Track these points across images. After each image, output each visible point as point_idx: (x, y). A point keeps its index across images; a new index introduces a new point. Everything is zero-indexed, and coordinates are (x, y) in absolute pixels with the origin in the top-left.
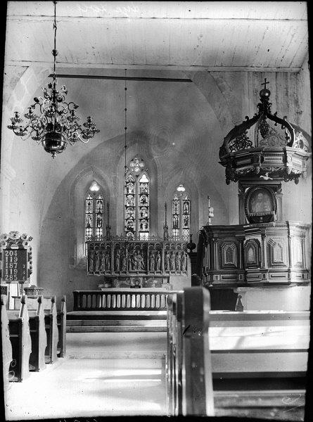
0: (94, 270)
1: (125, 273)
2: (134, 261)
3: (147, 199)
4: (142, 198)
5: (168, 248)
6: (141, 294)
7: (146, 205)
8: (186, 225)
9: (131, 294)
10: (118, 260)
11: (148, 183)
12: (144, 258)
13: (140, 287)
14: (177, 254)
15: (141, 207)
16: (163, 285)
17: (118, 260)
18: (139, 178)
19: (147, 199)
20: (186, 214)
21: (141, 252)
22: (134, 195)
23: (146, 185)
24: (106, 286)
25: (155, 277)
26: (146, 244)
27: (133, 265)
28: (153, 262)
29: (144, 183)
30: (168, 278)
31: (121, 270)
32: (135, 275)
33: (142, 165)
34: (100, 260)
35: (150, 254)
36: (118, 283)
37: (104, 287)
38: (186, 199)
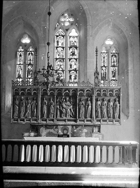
0: (19, 116)
1: (53, 120)
2: (63, 108)
3: (76, 52)
4: (71, 50)
5: (99, 95)
6: (70, 144)
7: (75, 57)
8: (114, 76)
9: (57, 144)
10: (45, 108)
11: (77, 37)
12: (73, 105)
13: (68, 136)
14: (109, 101)
15: (70, 59)
16: (94, 135)
17: (45, 108)
18: (69, 31)
19: (76, 52)
20: (114, 66)
21: (70, 99)
22: (63, 48)
23: (76, 38)
24: (32, 134)
25: (85, 126)
26: (75, 90)
27: (61, 112)
28: (83, 109)
29: (74, 37)
30: (99, 127)
31: (48, 117)
32: (63, 123)
33: (72, 20)
34: (26, 107)
35: (80, 100)
36: (43, 131)
37: (29, 136)
38: (114, 52)
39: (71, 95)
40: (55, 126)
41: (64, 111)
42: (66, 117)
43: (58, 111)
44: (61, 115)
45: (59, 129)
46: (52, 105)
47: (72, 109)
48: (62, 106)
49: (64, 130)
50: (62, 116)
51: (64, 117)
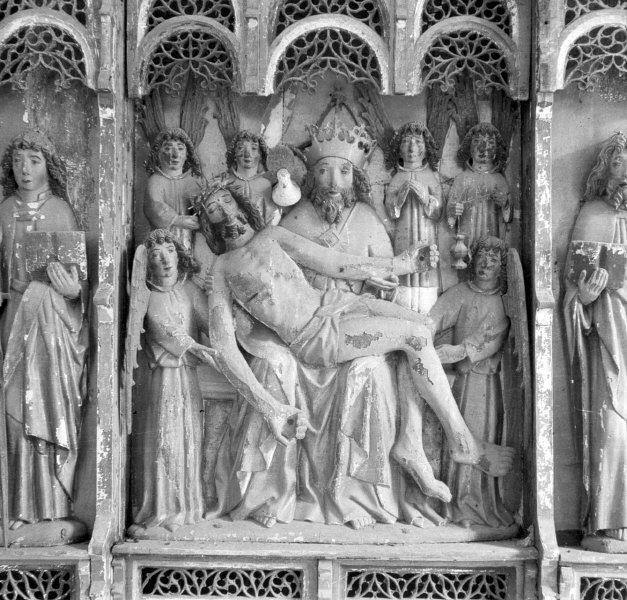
27: (228, 413)
39: (412, 84)
41: (279, 385)
42: (328, 502)
43: (174, 382)
44: (234, 462)
46: (36, 289)
47: (432, 361)
48: (245, 298)
50: (253, 488)
51: (287, 506)
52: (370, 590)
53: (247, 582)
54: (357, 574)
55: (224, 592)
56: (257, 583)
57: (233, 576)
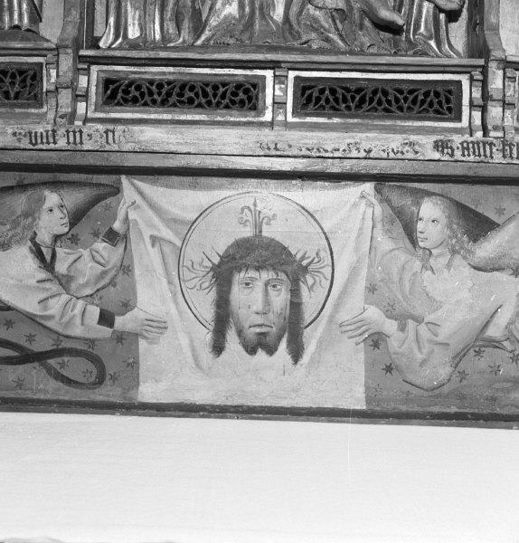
40: (75, 198)
45: (147, 259)
49: (223, 274)
52: (323, 102)
53: (205, 95)
54: (310, 87)
55: (182, 102)
56: (215, 95)
57: (192, 88)
